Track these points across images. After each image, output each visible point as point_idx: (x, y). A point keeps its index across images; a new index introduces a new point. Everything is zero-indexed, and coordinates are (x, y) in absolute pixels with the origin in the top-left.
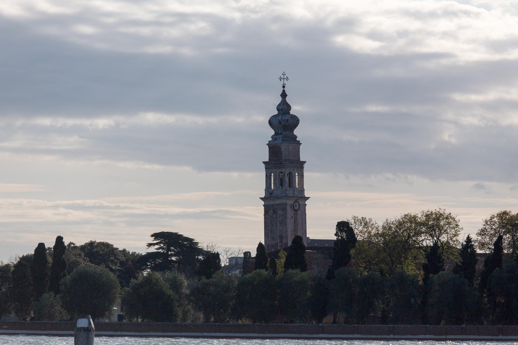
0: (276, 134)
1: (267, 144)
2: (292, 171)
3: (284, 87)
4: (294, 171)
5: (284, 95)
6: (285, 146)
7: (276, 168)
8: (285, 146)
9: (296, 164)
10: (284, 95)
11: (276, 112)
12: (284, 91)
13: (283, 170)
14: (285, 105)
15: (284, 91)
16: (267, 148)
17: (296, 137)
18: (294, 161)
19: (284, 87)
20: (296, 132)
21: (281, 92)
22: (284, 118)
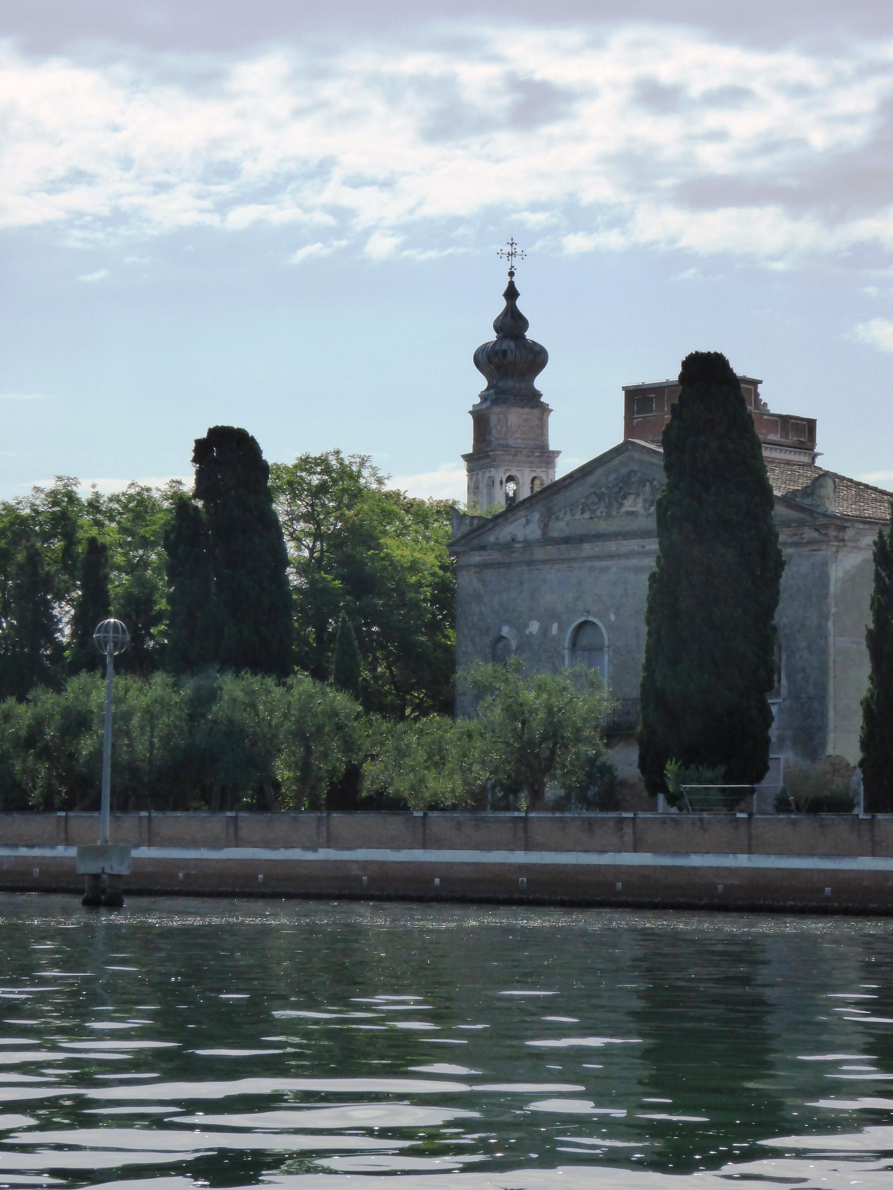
0: (488, 389)
1: (470, 412)
3: (511, 274)
4: (523, 476)
5: (511, 294)
6: (499, 414)
7: (481, 469)
8: (499, 414)
9: (529, 456)
10: (511, 294)
12: (511, 285)
13: (493, 472)
14: (509, 315)
15: (511, 285)
16: (470, 421)
17: (538, 395)
18: (519, 449)
19: (511, 274)
20: (541, 382)
21: (505, 286)
22: (497, 348)
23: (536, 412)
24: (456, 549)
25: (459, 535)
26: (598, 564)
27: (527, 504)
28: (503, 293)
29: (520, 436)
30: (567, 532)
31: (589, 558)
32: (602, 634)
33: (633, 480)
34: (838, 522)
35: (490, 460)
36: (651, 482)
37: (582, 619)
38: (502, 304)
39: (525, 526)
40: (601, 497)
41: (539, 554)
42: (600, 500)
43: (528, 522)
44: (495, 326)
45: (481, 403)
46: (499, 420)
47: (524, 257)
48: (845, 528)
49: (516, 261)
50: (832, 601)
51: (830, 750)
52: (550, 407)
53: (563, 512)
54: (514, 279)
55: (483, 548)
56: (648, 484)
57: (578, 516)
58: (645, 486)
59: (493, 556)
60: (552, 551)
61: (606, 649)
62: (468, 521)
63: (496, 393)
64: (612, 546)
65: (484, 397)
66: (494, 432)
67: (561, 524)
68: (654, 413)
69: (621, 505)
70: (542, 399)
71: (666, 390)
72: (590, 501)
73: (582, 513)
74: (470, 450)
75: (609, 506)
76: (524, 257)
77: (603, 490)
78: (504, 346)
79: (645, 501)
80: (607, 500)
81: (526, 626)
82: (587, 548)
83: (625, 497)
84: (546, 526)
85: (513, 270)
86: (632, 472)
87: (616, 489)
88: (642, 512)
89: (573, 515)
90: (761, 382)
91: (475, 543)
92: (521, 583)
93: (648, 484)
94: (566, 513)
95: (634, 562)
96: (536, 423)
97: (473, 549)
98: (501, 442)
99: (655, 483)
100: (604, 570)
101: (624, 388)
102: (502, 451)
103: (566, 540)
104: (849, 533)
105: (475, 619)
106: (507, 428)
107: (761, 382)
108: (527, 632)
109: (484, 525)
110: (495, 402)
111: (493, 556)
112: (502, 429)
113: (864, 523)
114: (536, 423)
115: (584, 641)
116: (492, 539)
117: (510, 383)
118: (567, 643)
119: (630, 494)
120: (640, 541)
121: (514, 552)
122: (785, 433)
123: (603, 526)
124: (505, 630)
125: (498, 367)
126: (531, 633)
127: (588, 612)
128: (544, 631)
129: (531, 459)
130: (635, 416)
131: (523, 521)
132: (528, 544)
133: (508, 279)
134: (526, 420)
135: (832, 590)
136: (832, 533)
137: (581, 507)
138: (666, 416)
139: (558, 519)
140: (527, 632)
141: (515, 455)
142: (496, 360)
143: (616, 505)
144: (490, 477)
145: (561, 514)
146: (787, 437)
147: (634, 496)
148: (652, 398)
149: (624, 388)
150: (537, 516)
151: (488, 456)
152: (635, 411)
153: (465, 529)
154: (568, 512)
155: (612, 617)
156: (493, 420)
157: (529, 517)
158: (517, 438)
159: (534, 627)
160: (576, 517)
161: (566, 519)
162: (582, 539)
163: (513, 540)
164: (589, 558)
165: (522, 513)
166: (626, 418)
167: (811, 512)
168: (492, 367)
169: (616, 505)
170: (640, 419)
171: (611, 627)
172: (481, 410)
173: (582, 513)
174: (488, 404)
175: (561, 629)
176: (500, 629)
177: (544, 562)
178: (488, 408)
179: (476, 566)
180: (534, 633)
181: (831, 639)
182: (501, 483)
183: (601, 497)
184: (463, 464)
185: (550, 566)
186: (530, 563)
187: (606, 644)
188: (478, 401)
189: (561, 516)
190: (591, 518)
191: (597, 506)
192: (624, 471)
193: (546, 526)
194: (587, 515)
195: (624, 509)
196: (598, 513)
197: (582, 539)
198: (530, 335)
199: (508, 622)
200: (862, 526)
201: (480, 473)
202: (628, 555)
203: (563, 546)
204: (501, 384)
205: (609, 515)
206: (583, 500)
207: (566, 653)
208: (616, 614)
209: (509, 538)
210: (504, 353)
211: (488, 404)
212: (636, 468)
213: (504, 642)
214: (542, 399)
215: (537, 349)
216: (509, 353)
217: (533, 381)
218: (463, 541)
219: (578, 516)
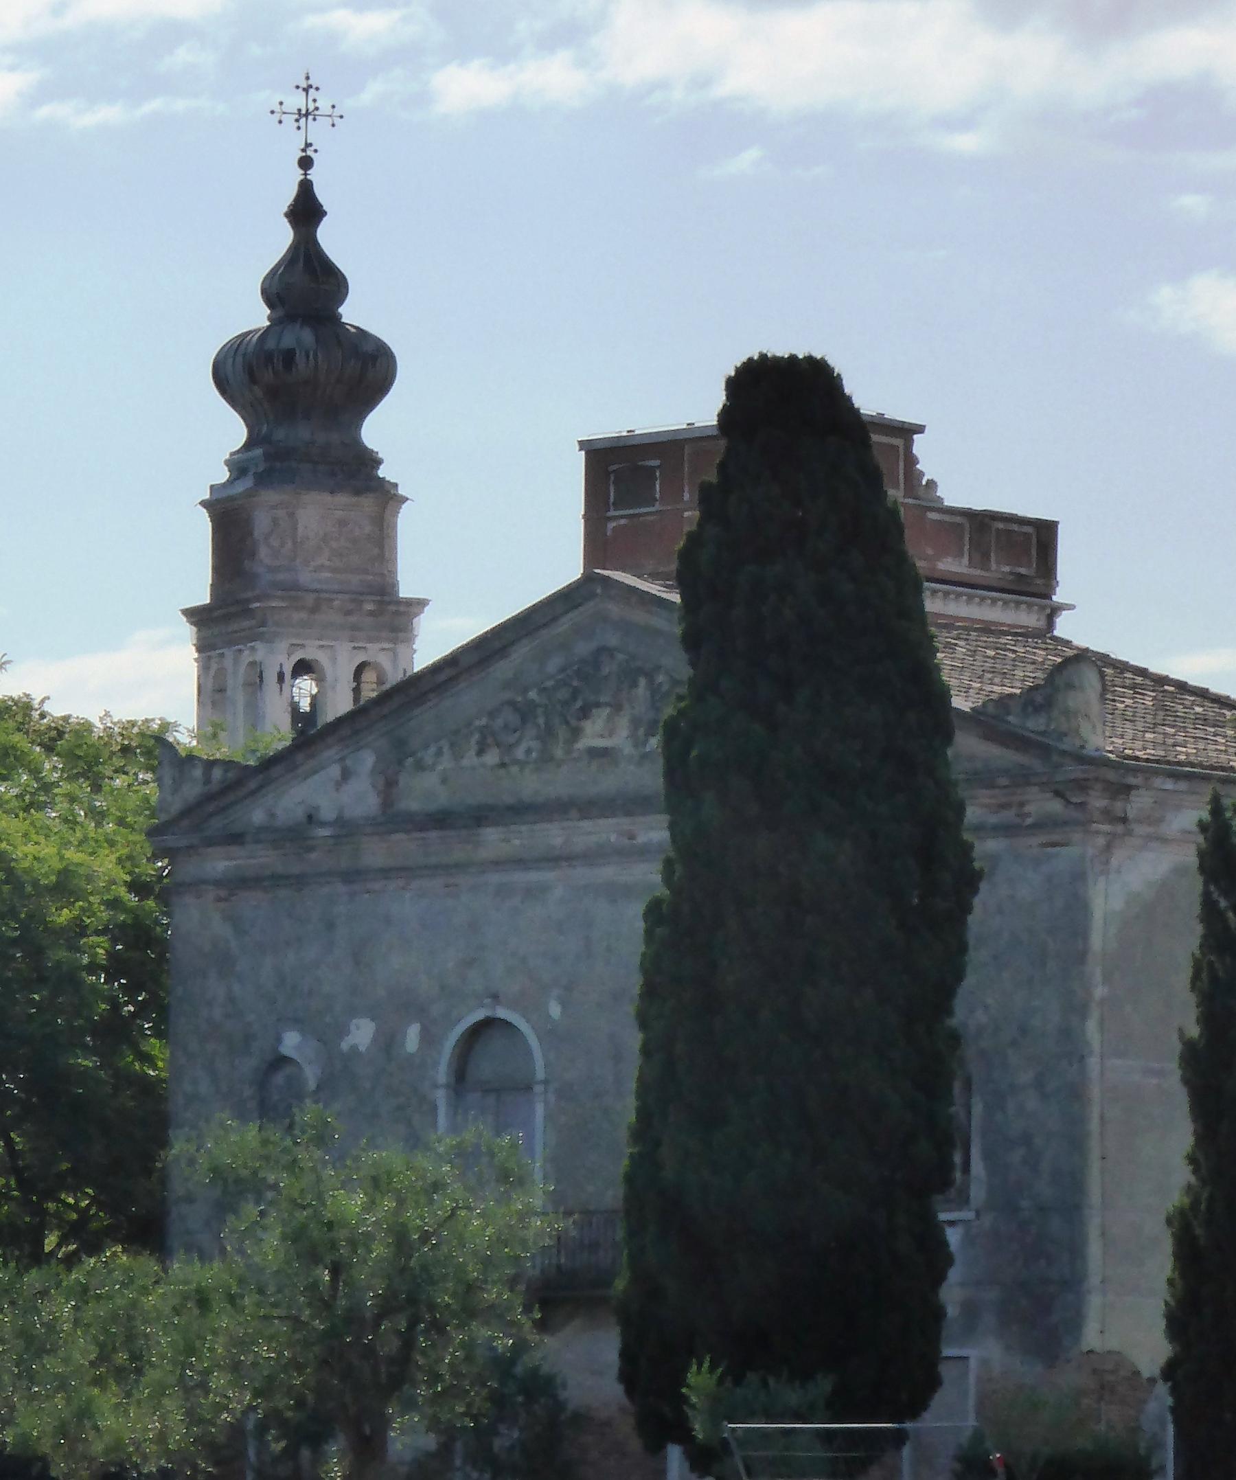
0: (248, 446)
1: (204, 504)
2: (322, 657)
3: (306, 163)
4: (334, 660)
6: (274, 507)
7: (230, 643)
8: (274, 507)
9: (348, 613)
11: (258, 316)
12: (306, 188)
13: (261, 652)
14: (301, 264)
15: (306, 188)
16: (203, 526)
17: (373, 461)
19: (306, 163)
22: (271, 344)
23: (368, 503)
24: (170, 840)
25: (177, 806)
26: (521, 877)
27: (345, 731)
28: (285, 209)
29: (327, 563)
30: (443, 799)
31: (497, 864)
32: (529, 1052)
33: (606, 670)
34: (1111, 775)
35: (254, 622)
36: (650, 676)
37: (479, 1015)
38: (283, 237)
39: (338, 785)
40: (526, 713)
41: (375, 853)
42: (524, 720)
43: (346, 775)
44: (264, 292)
45: (230, 482)
46: (275, 521)
47: (337, 120)
48: (1128, 789)
49: (317, 131)
50: (1095, 970)
51: (1091, 1338)
52: (401, 491)
53: (432, 750)
54: (313, 175)
55: (236, 839)
56: (642, 682)
57: (470, 759)
58: (634, 684)
59: (262, 858)
60: (405, 845)
61: (538, 1089)
62: (198, 773)
63: (267, 456)
64: (553, 835)
65: (238, 467)
66: (263, 552)
67: (429, 781)
68: (657, 507)
69: (576, 733)
70: (381, 473)
71: (687, 450)
72: (499, 722)
73: (480, 752)
74: (203, 597)
75: (547, 735)
76: (337, 120)
77: (532, 694)
78: (288, 341)
79: (635, 723)
80: (541, 721)
81: (343, 1031)
82: (493, 839)
83: (585, 713)
84: (391, 784)
85: (310, 152)
86: (603, 651)
87: (563, 694)
88: (628, 749)
89: (458, 756)
90: (920, 429)
91: (216, 824)
92: (330, 926)
93: (642, 682)
94: (439, 753)
95: (608, 872)
96: (368, 529)
97: (210, 842)
98: (281, 577)
99: (661, 678)
100: (533, 893)
101: (583, 445)
102: (282, 599)
103: (441, 820)
104: (1139, 803)
105: (217, 1013)
106: (295, 543)
107: (920, 429)
108: (345, 1046)
109: (238, 783)
110: (265, 479)
111: (262, 858)
112: (282, 545)
113: (1175, 776)
114: (368, 529)
115: (485, 1067)
116: (258, 816)
117: (302, 433)
118: (442, 1073)
119: (598, 705)
120: (624, 822)
121: (311, 849)
122: (981, 556)
123: (531, 785)
124: (291, 1042)
125: (273, 393)
126: (354, 1048)
127: (495, 997)
128: (388, 1042)
129: (352, 619)
130: (612, 513)
131: (335, 771)
132: (346, 829)
133: (298, 175)
134: (342, 523)
135: (1096, 941)
136: (1097, 802)
137: (477, 736)
138: (686, 514)
139: (420, 767)
140: (345, 1046)
141: (314, 610)
142: (268, 376)
143: (562, 733)
144: (253, 664)
145: (428, 756)
146: (985, 565)
147: (607, 710)
148: (653, 468)
149: (583, 445)
150: (368, 759)
151: (247, 613)
152: (612, 499)
153: (191, 791)
154: (446, 749)
155: (555, 1010)
156: (262, 522)
157: (348, 762)
158: (321, 568)
159: (362, 1034)
160: (465, 762)
161: (440, 768)
162: (481, 816)
163: (310, 818)
164: (497, 864)
165: (332, 753)
166: (587, 517)
167: (1044, 751)
168: (258, 391)
169: (562, 733)
170: (623, 522)
171: (552, 1036)
172: (232, 499)
173: (480, 752)
174: (247, 483)
175: (429, 1039)
176: (279, 1040)
177: (386, 873)
178: (249, 494)
179: (218, 883)
180: (362, 1049)
181: (1093, 1062)
182: (281, 677)
183: (526, 713)
184: (187, 632)
185: (401, 882)
186: (352, 876)
187: (540, 1074)
188: (223, 475)
189: (429, 760)
190: (503, 765)
191: (517, 734)
192: (583, 648)
193: (391, 784)
194: (492, 757)
195: (582, 744)
196: (520, 753)
197: (481, 816)
198: (352, 313)
199: (297, 1022)
200: (1169, 785)
201: (229, 653)
202: (592, 857)
203: (433, 834)
204: (280, 434)
205: (546, 759)
206: (484, 721)
207: (441, 1097)
208: (564, 1004)
209: (300, 813)
210: (289, 357)
211: (247, 483)
212: (613, 640)
213: (288, 1070)
214: (381, 473)
215: (369, 348)
216: (299, 358)
217: (359, 426)
218: (185, 823)
219: (470, 759)
